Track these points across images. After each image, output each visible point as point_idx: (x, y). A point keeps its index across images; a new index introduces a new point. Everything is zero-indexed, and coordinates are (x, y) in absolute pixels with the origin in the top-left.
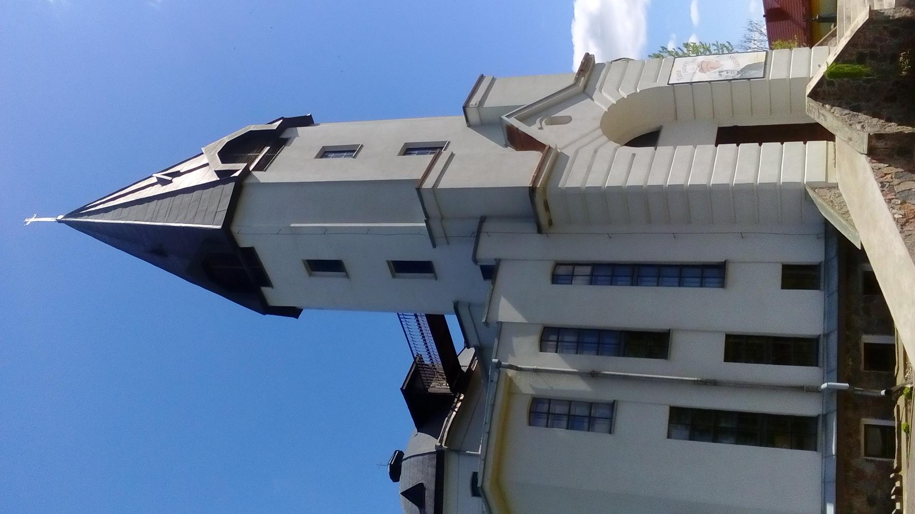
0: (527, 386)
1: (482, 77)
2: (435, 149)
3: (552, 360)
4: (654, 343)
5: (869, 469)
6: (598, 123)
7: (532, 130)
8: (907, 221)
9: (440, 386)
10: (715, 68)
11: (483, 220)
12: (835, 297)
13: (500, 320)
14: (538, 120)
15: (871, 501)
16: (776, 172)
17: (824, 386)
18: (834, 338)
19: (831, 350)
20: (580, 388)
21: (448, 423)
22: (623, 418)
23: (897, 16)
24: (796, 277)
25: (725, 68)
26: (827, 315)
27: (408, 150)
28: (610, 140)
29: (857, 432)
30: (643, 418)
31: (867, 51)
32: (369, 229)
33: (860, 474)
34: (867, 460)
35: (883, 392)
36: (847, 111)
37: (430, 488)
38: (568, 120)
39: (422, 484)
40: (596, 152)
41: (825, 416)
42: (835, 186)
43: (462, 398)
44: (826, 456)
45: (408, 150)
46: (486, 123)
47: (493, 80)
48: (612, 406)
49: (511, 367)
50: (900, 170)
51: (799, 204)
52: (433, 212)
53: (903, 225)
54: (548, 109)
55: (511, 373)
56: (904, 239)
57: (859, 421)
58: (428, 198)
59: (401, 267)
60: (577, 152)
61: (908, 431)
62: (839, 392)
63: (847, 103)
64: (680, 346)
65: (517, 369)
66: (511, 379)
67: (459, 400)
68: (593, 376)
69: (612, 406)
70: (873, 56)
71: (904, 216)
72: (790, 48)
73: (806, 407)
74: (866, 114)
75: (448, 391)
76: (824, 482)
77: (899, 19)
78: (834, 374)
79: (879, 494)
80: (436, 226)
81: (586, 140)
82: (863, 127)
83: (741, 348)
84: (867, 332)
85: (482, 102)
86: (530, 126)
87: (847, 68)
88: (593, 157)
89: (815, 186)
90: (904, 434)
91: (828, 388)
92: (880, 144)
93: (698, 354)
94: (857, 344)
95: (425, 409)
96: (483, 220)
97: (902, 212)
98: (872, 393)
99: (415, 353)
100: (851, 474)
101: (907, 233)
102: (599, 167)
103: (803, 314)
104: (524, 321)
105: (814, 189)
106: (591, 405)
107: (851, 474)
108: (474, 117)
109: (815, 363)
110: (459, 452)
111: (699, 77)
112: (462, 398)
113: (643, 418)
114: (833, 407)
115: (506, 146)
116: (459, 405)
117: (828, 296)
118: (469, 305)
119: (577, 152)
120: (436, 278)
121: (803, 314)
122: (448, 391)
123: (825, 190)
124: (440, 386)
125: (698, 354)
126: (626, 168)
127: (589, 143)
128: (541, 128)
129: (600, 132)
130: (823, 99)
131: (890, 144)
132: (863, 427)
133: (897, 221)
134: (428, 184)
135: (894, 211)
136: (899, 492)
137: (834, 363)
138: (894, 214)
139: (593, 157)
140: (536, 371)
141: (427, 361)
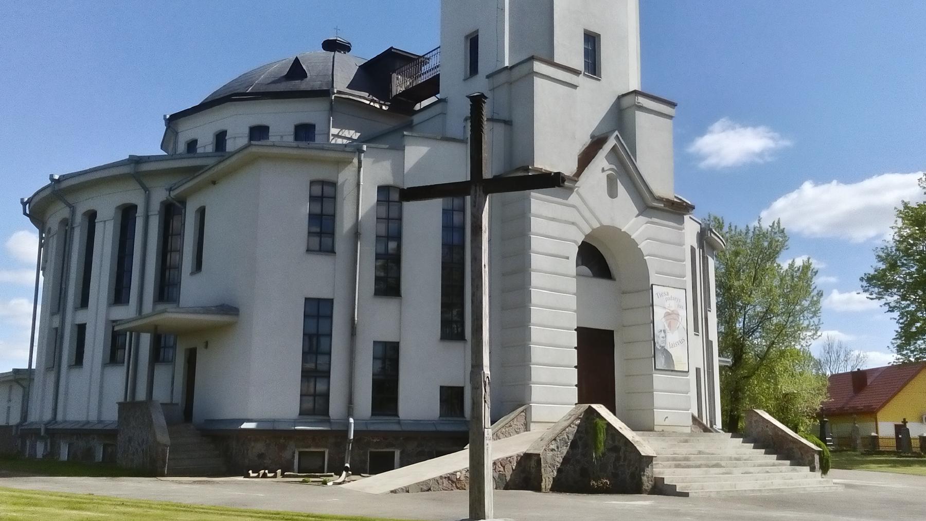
0: (345, 177)
1: (672, 105)
2: (593, 66)
3: (368, 199)
4: (389, 284)
5: (287, 454)
6: (606, 222)
7: (601, 162)
8: (453, 482)
9: (399, 84)
10: (669, 326)
11: (508, 123)
12: (432, 428)
13: (407, 148)
14: (614, 167)
15: (261, 456)
16: (543, 381)
17: (352, 420)
18: (396, 428)
19: (385, 424)
20: (345, 224)
21: (364, 97)
22: (321, 262)
23: (644, 479)
24: (452, 398)
25: (668, 335)
26: (417, 422)
27: (592, 40)
28: (586, 236)
29: (317, 446)
30: (320, 277)
31: (621, 454)
32: (503, 10)
33: (283, 448)
34: (294, 453)
35: (348, 465)
36: (571, 437)
37: (303, 85)
38: (613, 193)
39: (306, 76)
40: (573, 223)
41: (328, 421)
42: (527, 429)
43: (384, 107)
44: (296, 422)
45: (592, 40)
46: (620, 115)
47: (670, 117)
48: (332, 251)
49: (360, 162)
50: (508, 478)
51: (513, 401)
52: (516, 73)
53: (449, 478)
54: (626, 173)
55: (355, 161)
56: (434, 479)
57: (326, 447)
58: (524, 68)
59: (473, 42)
60: (574, 206)
61: (304, 482)
62: (347, 432)
63: (581, 438)
64: (388, 306)
65: (360, 167)
66: (351, 162)
67: (381, 105)
68: (356, 234)
69: (332, 251)
70: (618, 459)
71: (459, 480)
72: (100, 422)
73: (336, 407)
74: (568, 452)
75: (394, 93)
76: (274, 421)
77: (641, 479)
78: (359, 428)
79: (267, 462)
80: (502, 78)
81: (587, 214)
82: (552, 450)
83: (388, 356)
84: (401, 453)
85: (641, 108)
86: (606, 157)
87: (602, 437)
88: (566, 222)
89: (527, 412)
90: (301, 479)
91: (349, 424)
92: (533, 463)
93: (378, 320)
94: (392, 446)
95: (375, 73)
96: (508, 123)
97: (463, 478)
98: (348, 458)
99: (428, 56)
100: (282, 441)
101: (440, 481)
102: (554, 228)
103: (418, 401)
104: (406, 171)
105: (525, 411)
106: (332, 234)
107: (282, 441)
108: (626, 102)
109: (374, 413)
110: (332, 110)
111: (659, 313)
112: (384, 107)
113: (320, 277)
114: (335, 428)
115: (592, 137)
116: (377, 106)
117: (433, 423)
118: (444, 114)
119: (574, 206)
120: (464, 80)
121: (418, 401)
122: (394, 93)
123: (523, 421)
124: (399, 84)
125: (378, 320)
126: (552, 252)
127: (583, 217)
128: (603, 170)
129: (596, 225)
130: (587, 419)
131: (533, 471)
132: (322, 450)
133: (454, 474)
134: (538, 67)
135: (464, 472)
136: (264, 476)
137: (372, 428)
138: (460, 471)
139: (566, 222)
140: (358, 185)
141: (425, 68)
